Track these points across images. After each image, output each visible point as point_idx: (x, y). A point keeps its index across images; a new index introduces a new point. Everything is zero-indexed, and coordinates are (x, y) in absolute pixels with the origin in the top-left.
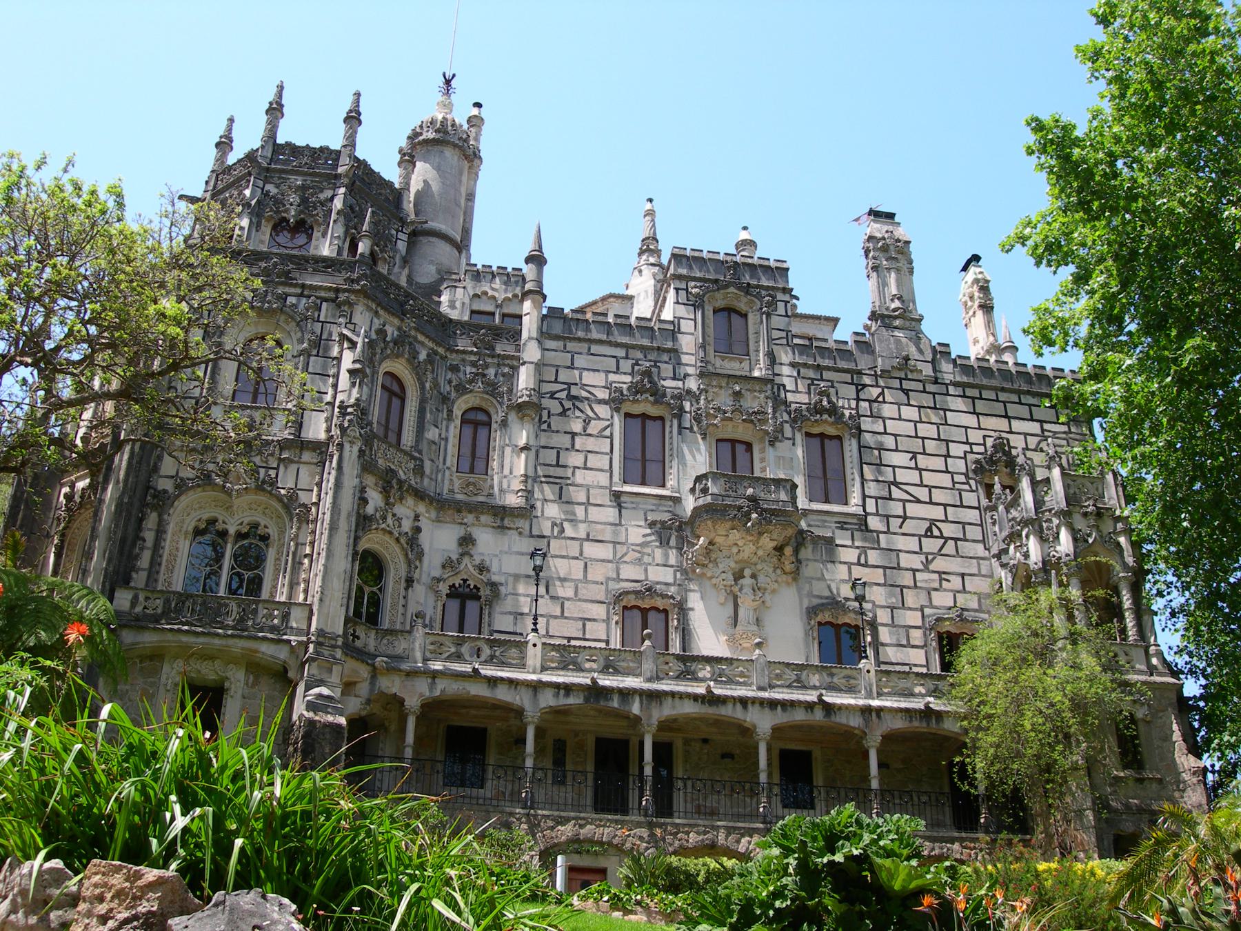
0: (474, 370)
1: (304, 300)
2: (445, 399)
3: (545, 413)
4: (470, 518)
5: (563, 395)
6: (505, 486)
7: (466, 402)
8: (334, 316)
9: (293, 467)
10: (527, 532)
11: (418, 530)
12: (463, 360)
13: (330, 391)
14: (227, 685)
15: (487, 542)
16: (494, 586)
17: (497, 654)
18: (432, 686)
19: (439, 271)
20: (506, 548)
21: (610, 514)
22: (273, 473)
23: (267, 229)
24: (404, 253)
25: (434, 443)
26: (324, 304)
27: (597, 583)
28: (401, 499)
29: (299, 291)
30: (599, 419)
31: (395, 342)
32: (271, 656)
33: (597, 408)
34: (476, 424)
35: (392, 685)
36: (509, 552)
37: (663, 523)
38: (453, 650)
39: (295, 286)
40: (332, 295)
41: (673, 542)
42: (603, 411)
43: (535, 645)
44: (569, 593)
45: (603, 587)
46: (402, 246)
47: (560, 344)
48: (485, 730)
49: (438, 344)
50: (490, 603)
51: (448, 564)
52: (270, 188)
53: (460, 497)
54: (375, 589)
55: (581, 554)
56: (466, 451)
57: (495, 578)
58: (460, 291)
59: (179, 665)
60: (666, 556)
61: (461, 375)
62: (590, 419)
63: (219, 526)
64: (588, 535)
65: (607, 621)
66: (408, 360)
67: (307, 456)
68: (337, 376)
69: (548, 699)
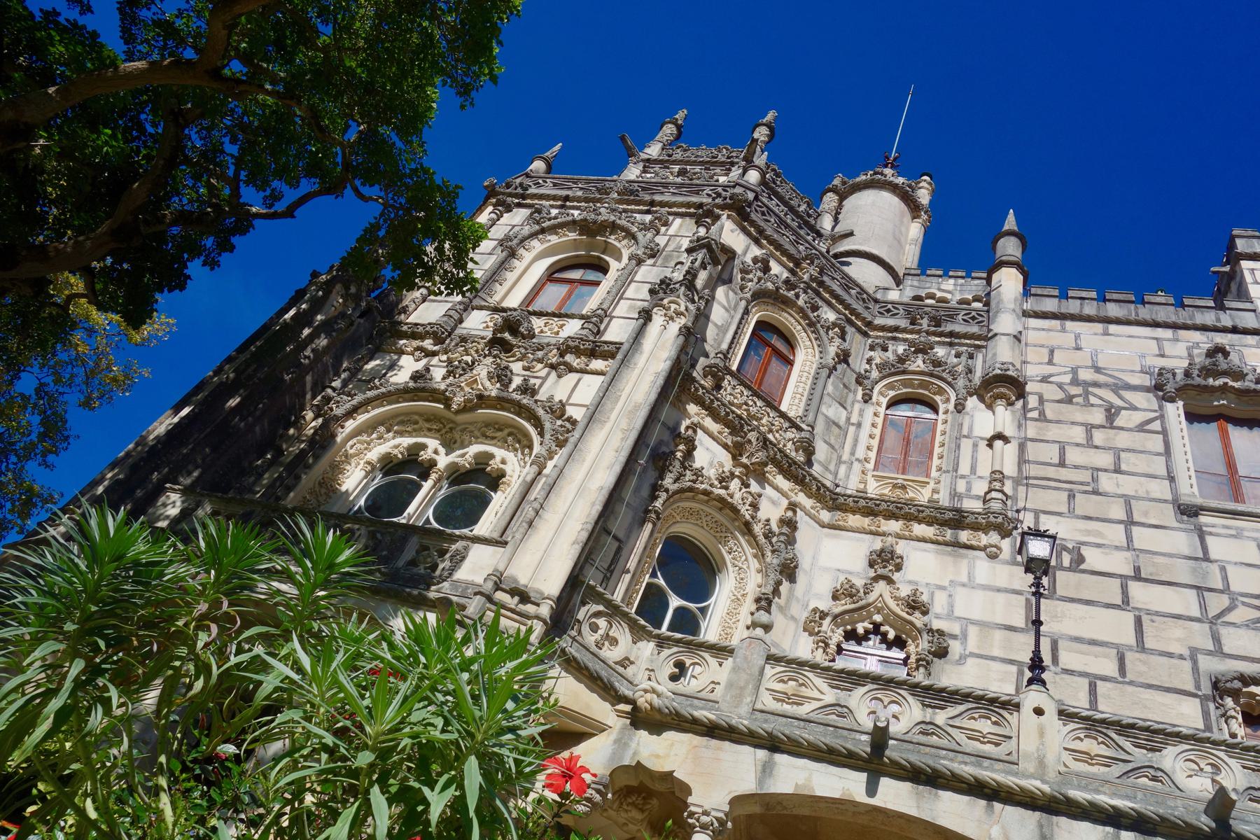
2: (860, 379)
3: (1033, 401)
4: (894, 526)
5: (1067, 379)
7: (890, 386)
9: (573, 377)
11: (790, 524)
18: (766, 770)
20: (964, 579)
21: (1180, 541)
26: (678, 221)
27: (1170, 655)
30: (1133, 408)
33: (1128, 395)
35: (665, 752)
36: (970, 584)
42: (1140, 399)
44: (1108, 667)
47: (1056, 323)
54: (692, 606)
57: (936, 625)
62: (1120, 409)
64: (1137, 570)
66: (801, 310)
67: (598, 364)
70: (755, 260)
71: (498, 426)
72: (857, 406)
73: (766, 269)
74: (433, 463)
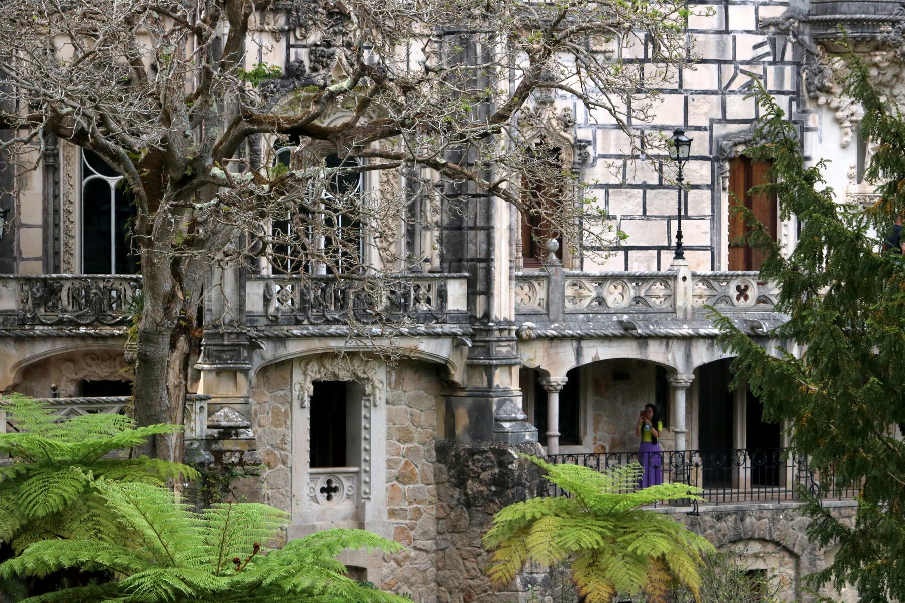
16: (580, 146)
17: (642, 295)
18: (579, 353)
32: (431, 355)
37: (776, 24)
38: (594, 294)
41: (789, 56)
43: (684, 279)
45: (707, 134)
55: (681, 86)
59: (315, 372)
60: (780, 77)
65: (711, 187)
69: (702, 355)
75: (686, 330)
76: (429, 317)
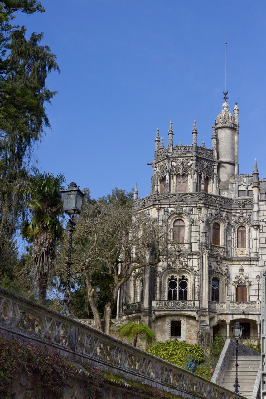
0: (240, 215)
1: (188, 208)
3: (261, 226)
4: (242, 263)
6: (251, 251)
8: (197, 212)
9: (191, 260)
10: (258, 265)
11: (227, 270)
12: (236, 212)
13: (198, 236)
14: (182, 322)
15: (247, 268)
16: (249, 282)
18: (233, 317)
19: (228, 176)
22: (186, 263)
23: (175, 178)
24: (216, 173)
25: (230, 241)
26: (194, 208)
28: (221, 263)
29: (186, 206)
31: (216, 215)
34: (242, 231)
38: (237, 306)
39: (185, 204)
40: (195, 205)
43: (258, 303)
46: (215, 171)
48: (250, 323)
49: (228, 209)
50: (249, 287)
51: (237, 277)
52: (173, 163)
53: (239, 256)
56: (240, 240)
57: (250, 280)
58: (234, 185)
61: (236, 217)
63: (175, 278)
67: (194, 257)
68: (199, 232)
70: (209, 214)
71: (184, 271)
72: (232, 233)
73: (212, 214)
74: (176, 280)
75: (258, 313)
76: (190, 308)
